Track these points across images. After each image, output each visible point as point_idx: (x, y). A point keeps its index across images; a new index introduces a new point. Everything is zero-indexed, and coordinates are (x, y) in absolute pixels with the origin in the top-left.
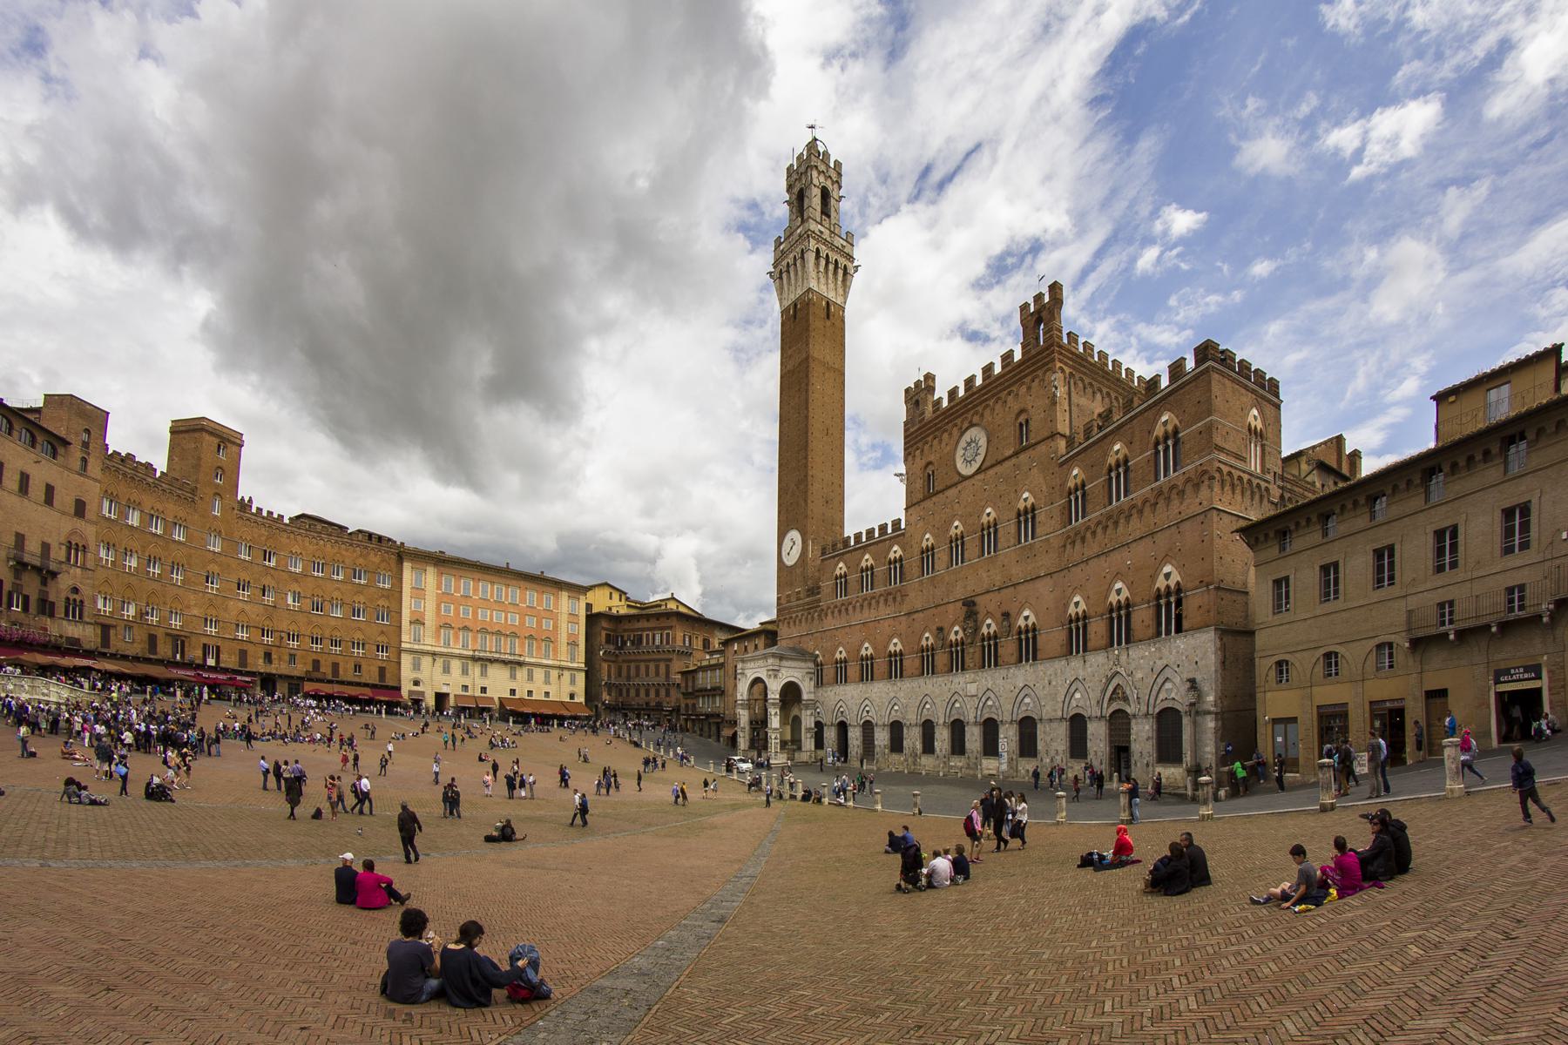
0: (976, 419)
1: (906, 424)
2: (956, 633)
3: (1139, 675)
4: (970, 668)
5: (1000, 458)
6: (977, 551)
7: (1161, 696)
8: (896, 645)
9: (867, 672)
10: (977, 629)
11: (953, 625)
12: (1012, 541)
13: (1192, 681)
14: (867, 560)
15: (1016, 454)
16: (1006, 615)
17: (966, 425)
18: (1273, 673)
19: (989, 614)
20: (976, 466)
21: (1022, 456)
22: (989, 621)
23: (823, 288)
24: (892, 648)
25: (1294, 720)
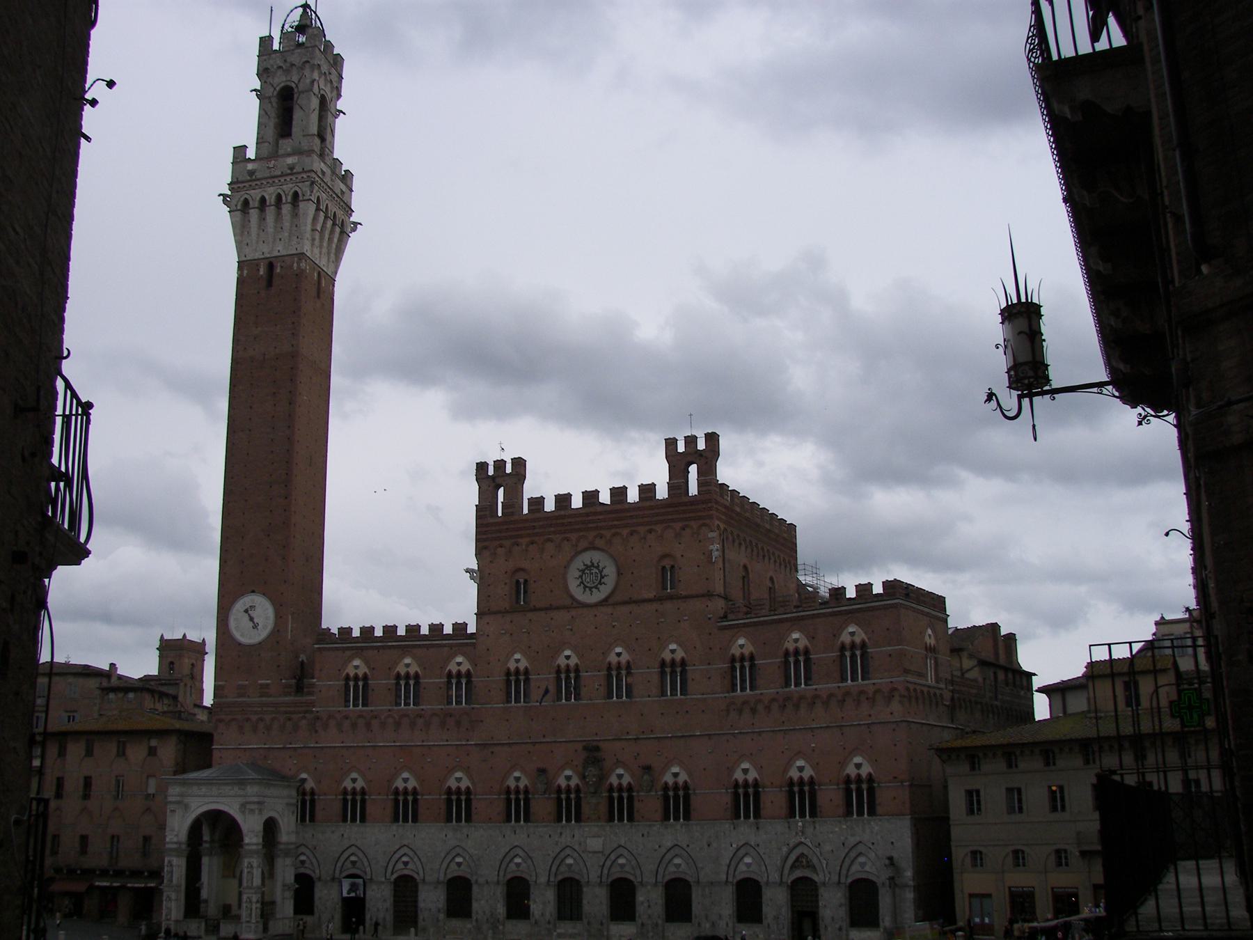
2: (567, 777)
3: (827, 847)
7: (855, 867)
8: (459, 780)
9: (405, 808)
10: (602, 777)
11: (562, 768)
13: (891, 858)
14: (408, 664)
15: (659, 599)
16: (648, 769)
18: (968, 860)
19: (619, 763)
20: (597, 597)
21: (669, 606)
22: (620, 771)
23: (316, 251)
24: (452, 784)
25: (989, 896)
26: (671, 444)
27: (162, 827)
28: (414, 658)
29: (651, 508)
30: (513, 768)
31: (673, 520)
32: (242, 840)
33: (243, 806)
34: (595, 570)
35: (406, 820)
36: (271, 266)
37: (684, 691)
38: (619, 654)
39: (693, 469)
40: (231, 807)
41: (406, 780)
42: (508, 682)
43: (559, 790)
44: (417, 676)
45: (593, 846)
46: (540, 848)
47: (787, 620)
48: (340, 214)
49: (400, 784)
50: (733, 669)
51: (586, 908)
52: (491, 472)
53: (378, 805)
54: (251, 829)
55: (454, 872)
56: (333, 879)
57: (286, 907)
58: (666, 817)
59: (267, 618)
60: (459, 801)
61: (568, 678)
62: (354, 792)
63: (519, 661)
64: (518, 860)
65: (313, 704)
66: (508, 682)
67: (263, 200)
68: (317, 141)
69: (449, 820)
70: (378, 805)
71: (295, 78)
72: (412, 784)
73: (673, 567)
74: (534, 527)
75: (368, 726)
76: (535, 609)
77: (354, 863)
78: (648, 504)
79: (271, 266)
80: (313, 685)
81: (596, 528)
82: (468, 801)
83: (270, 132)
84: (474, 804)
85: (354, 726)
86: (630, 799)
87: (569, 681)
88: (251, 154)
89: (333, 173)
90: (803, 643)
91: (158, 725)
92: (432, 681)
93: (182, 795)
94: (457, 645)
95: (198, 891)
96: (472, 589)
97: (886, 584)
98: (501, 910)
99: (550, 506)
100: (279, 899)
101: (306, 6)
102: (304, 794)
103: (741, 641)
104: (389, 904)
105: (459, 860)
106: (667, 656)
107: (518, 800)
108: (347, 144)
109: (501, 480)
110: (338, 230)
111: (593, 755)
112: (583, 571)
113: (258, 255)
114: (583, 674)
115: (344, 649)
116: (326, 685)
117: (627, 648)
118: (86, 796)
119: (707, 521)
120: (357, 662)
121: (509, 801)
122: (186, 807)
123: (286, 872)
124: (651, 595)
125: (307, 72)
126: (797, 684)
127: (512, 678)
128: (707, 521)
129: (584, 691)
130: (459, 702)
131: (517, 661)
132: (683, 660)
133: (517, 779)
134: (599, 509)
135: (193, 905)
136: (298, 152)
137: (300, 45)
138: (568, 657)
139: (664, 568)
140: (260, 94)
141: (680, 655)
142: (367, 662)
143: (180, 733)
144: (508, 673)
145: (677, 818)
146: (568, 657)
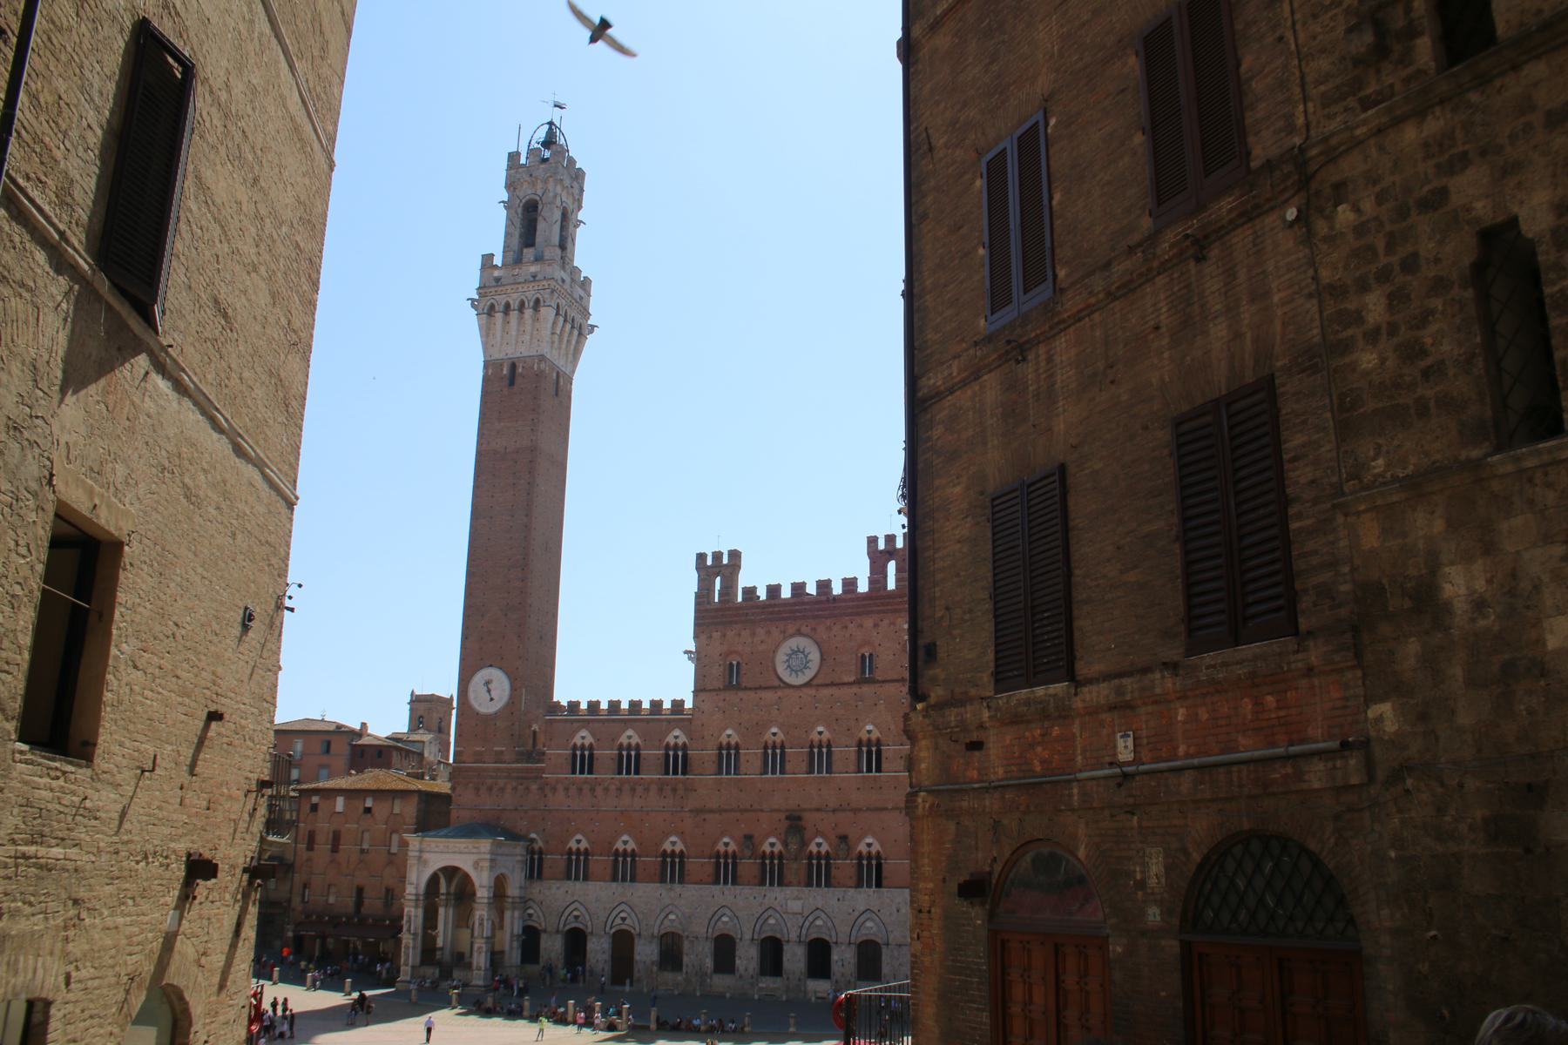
0: (804, 629)
1: (698, 596)
2: (771, 844)
4: (789, 884)
5: (837, 681)
8: (673, 843)
9: (624, 868)
10: (804, 844)
11: (768, 836)
12: (852, 768)
14: (630, 736)
15: (861, 681)
16: (844, 838)
17: (791, 630)
19: (818, 833)
21: (867, 690)
22: (819, 840)
23: (555, 352)
24: (667, 847)
26: (872, 541)
27: (403, 878)
29: (852, 600)
30: (723, 835)
32: (474, 894)
33: (476, 865)
35: (624, 879)
36: (513, 366)
37: (879, 770)
39: (892, 567)
40: (465, 863)
41: (625, 843)
42: (720, 755)
43: (763, 856)
44: (638, 747)
45: (794, 909)
46: (747, 908)
48: (578, 319)
49: (620, 846)
51: (786, 964)
52: (709, 562)
53: (600, 862)
54: (482, 883)
55: (668, 927)
56: (557, 932)
57: (514, 956)
58: (859, 885)
60: (673, 863)
62: (578, 852)
63: (730, 735)
64: (725, 919)
66: (720, 755)
67: (507, 306)
68: (558, 251)
69: (662, 880)
70: (600, 862)
71: (540, 192)
72: (631, 846)
75: (593, 790)
76: (746, 689)
77: (576, 917)
79: (513, 366)
82: (682, 863)
83: (516, 240)
84: (687, 867)
85: (580, 790)
86: (828, 865)
87: (774, 758)
88: (498, 261)
89: (573, 280)
91: (401, 786)
92: (652, 754)
93: (421, 851)
95: (434, 938)
96: (691, 667)
98: (709, 963)
99: (762, 594)
100: (507, 948)
101: (551, 123)
102: (533, 853)
104: (607, 956)
105: (672, 917)
106: (865, 737)
107: (726, 864)
108: (587, 254)
109: (717, 570)
110: (576, 332)
111: (795, 824)
113: (502, 356)
115: (572, 721)
116: (557, 753)
117: (828, 726)
118: (335, 849)
120: (584, 733)
121: (718, 864)
122: (425, 863)
123: (513, 923)
124: (852, 679)
125: (551, 186)
129: (788, 767)
130: (675, 772)
132: (878, 740)
133: (726, 844)
134: (806, 599)
135: (429, 952)
136: (539, 259)
137: (545, 160)
140: (508, 205)
141: (876, 735)
142: (593, 735)
143: (419, 792)
144: (720, 748)
145: (869, 886)
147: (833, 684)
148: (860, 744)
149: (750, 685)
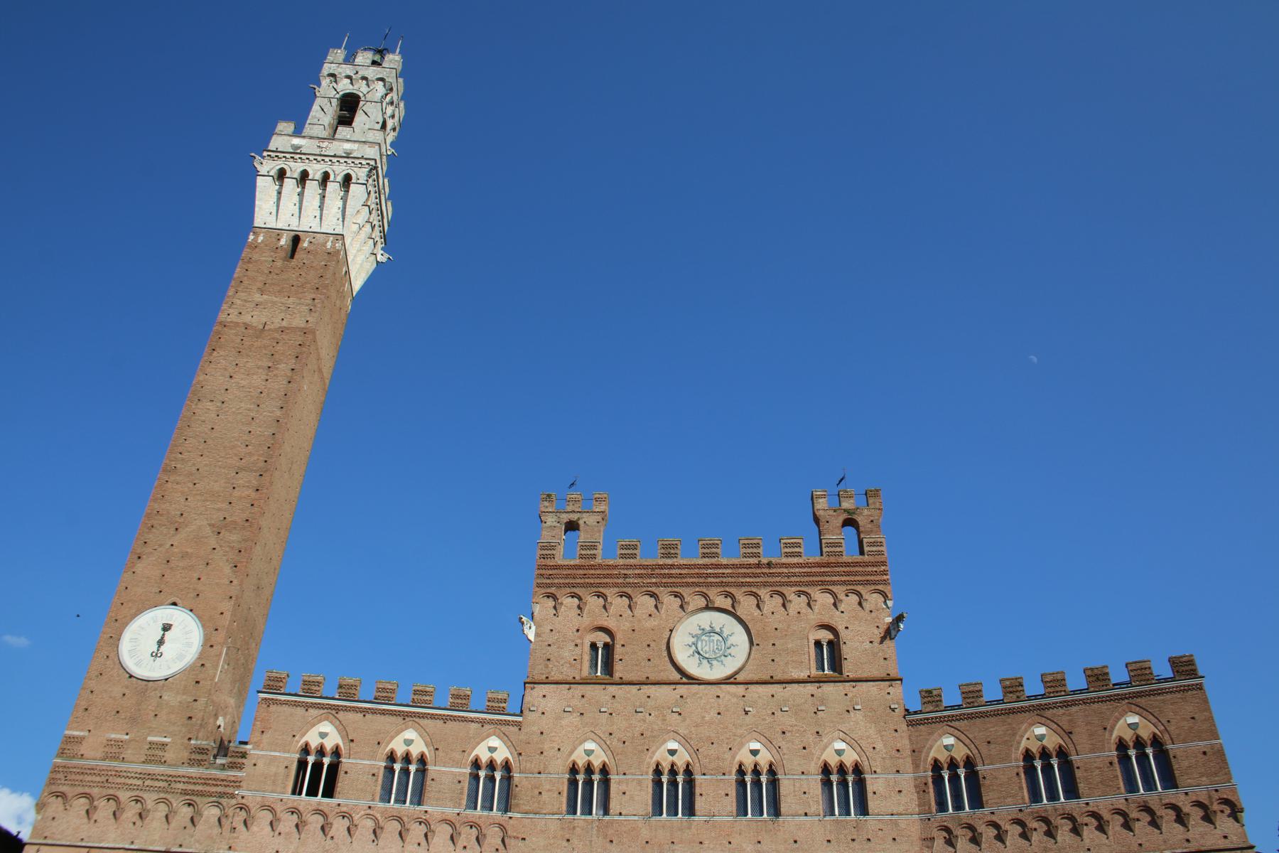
5: (778, 677)
6: (731, 803)
14: (409, 741)
15: (819, 681)
21: (828, 688)
28: (423, 732)
31: (834, 583)
34: (717, 637)
36: (296, 240)
37: (863, 809)
38: (754, 751)
44: (422, 760)
47: (1022, 710)
50: (938, 780)
59: (189, 645)
61: (673, 783)
63: (591, 751)
65: (237, 783)
66: (573, 783)
67: (304, 176)
73: (830, 643)
74: (626, 576)
76: (622, 683)
78: (795, 560)
79: (296, 240)
80: (244, 755)
81: (721, 584)
90: (1052, 742)
92: (448, 774)
94: (491, 722)
97: (1174, 662)
103: (949, 740)
106: (833, 762)
112: (697, 637)
114: (698, 778)
119: (880, 587)
120: (326, 727)
124: (803, 675)
126: (1053, 796)
127: (581, 778)
128: (880, 587)
129: (699, 804)
131: (589, 753)
138: (672, 752)
139: (818, 644)
141: (850, 758)
142: (343, 730)
144: (574, 770)
146: (671, 750)
147: (771, 682)
148: (826, 770)
149: (627, 677)
